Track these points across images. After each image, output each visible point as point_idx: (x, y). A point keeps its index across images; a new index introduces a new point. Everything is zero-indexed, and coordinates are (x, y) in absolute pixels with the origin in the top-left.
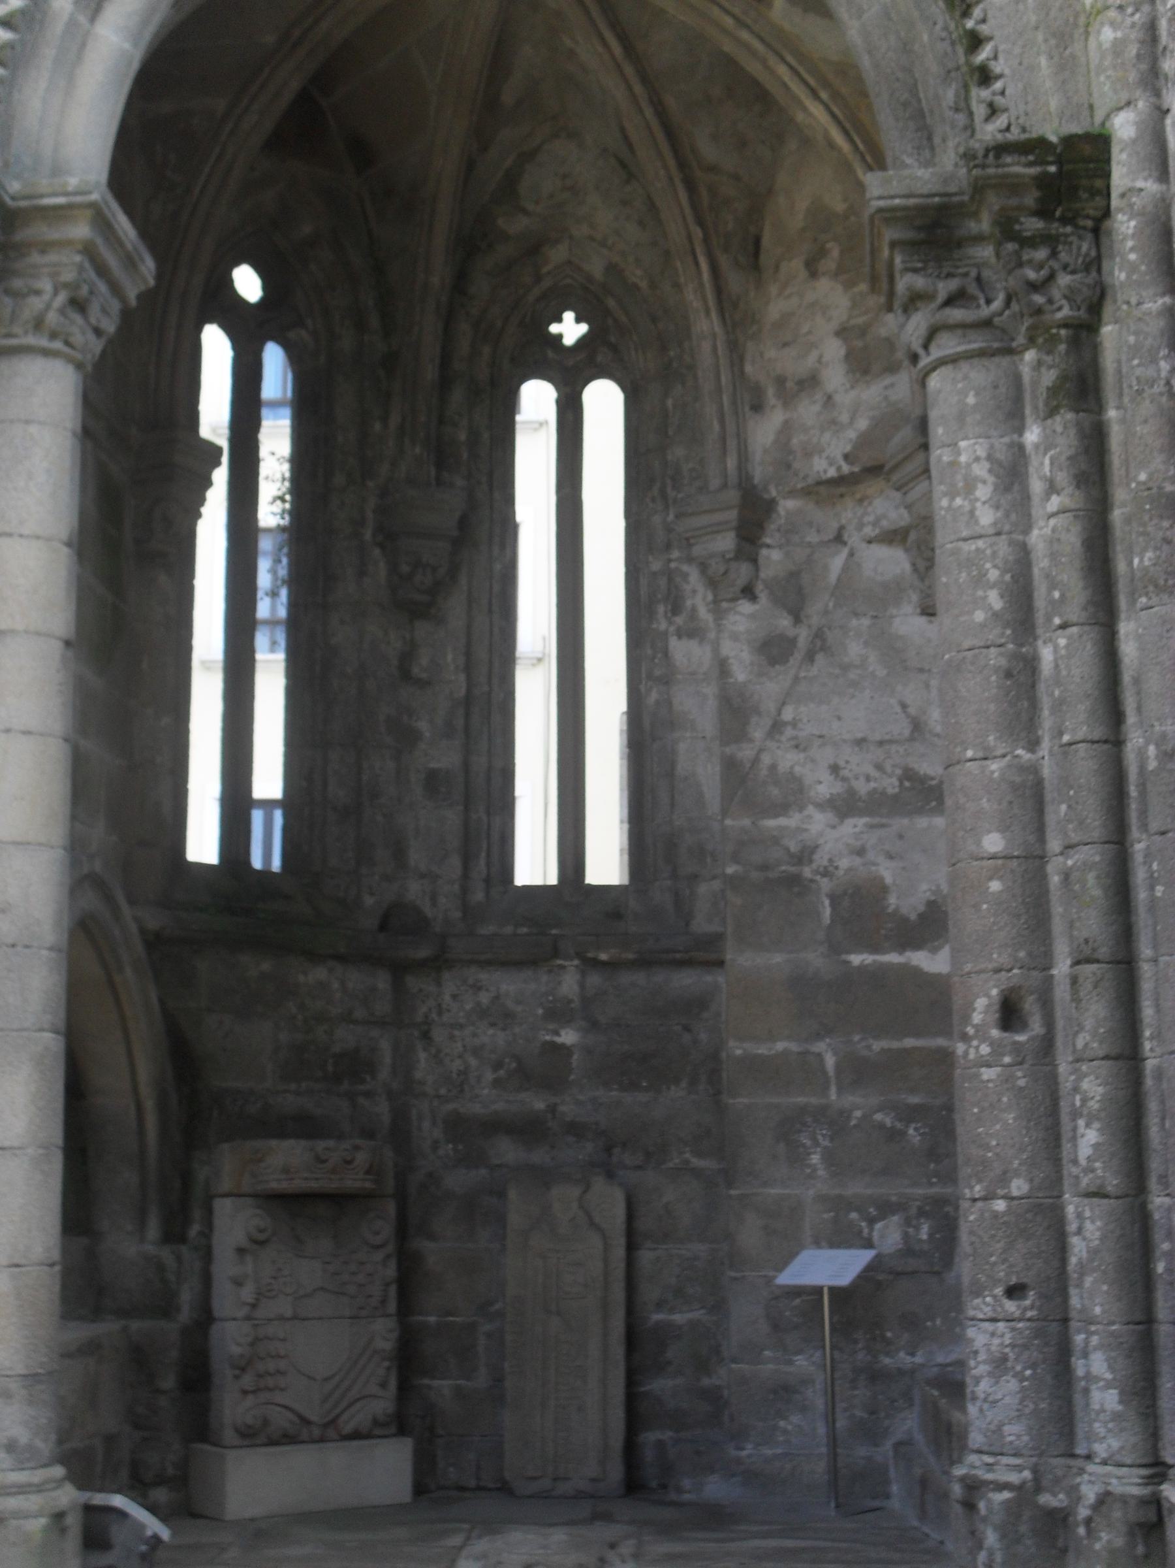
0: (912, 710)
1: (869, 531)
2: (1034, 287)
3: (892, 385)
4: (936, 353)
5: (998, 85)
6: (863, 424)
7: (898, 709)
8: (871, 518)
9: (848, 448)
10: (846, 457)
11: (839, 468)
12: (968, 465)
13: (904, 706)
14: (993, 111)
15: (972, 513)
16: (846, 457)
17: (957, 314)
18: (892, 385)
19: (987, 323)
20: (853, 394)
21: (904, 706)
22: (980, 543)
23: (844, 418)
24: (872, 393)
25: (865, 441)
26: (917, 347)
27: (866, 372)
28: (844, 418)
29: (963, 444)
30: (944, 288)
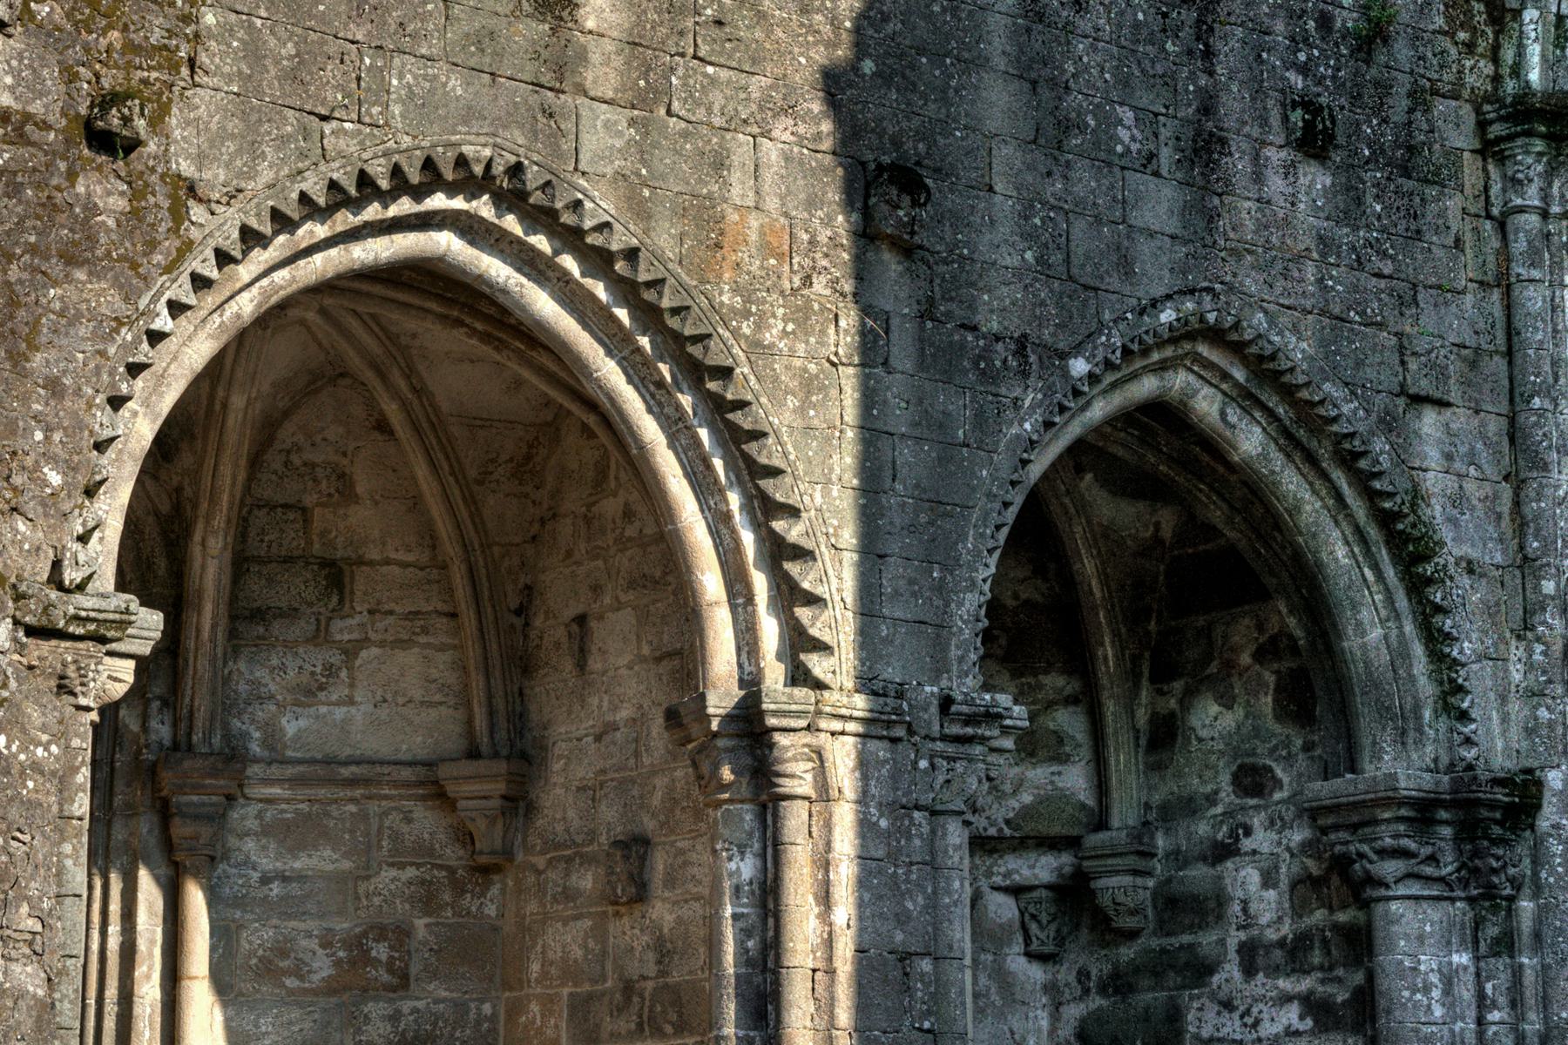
0: (1016, 1036)
1: (998, 880)
2: (1495, 871)
3: (1059, 773)
4: (1401, 890)
5: (1473, 727)
6: (1027, 798)
7: (1008, 1035)
8: (1002, 870)
9: (1011, 815)
10: (1007, 822)
11: (1001, 830)
12: (1427, 973)
13: (1012, 1033)
14: (1468, 741)
15: (1429, 1007)
16: (1007, 822)
17: (1428, 870)
18: (1059, 773)
19: (1441, 879)
20: (1016, 770)
21: (1012, 1033)
22: (1434, 1028)
23: (1008, 788)
24: (1038, 774)
25: (1026, 813)
26: (1390, 879)
27: (1032, 754)
28: (1008, 788)
29: (1423, 958)
30: (1426, 851)
